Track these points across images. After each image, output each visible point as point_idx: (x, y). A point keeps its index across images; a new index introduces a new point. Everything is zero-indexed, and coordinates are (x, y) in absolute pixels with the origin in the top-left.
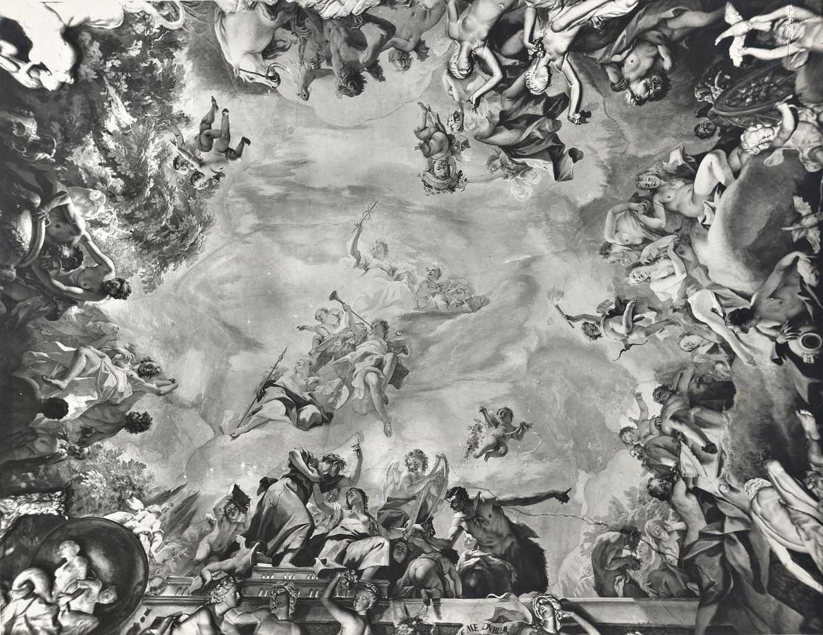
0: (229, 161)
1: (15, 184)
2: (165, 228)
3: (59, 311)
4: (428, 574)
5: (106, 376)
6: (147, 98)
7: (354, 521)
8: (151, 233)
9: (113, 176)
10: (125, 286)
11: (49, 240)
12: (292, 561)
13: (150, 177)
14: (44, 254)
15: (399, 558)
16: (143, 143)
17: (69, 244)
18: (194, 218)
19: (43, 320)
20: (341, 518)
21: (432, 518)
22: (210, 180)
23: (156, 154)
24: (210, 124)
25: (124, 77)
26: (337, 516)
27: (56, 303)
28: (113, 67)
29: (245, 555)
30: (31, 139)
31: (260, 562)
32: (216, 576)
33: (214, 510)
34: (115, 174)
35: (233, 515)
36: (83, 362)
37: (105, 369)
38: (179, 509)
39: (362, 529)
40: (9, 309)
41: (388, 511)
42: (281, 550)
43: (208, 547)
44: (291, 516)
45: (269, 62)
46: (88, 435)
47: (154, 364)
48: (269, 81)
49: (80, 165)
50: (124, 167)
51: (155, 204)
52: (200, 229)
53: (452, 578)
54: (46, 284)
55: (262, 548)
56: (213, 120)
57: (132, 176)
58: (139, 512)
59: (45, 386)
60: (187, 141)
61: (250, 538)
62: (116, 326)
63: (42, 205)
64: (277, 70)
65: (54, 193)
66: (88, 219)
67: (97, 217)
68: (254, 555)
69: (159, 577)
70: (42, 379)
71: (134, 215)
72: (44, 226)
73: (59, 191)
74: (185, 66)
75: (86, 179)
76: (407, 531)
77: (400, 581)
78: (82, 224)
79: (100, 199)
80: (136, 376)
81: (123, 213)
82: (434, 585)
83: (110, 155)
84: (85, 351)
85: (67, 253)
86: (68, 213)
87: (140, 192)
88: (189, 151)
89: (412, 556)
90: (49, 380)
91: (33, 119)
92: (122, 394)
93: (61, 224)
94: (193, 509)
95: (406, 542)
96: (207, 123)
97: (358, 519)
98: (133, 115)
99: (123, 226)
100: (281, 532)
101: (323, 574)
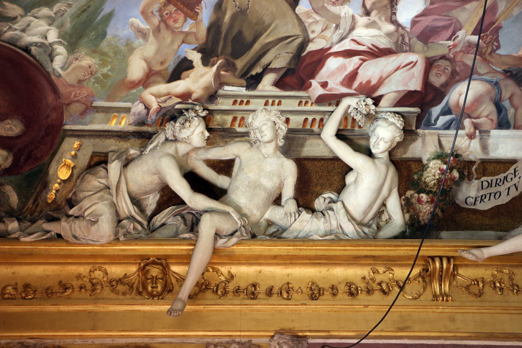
4: (478, 101)
7: (373, 31)
12: (278, 84)
15: (437, 80)
20: (352, 29)
21: (499, 28)
26: (345, 25)
29: (202, 76)
31: (228, 84)
32: (165, 101)
33: (143, 13)
35: (175, 21)
38: (84, 11)
39: (384, 43)
41: (430, 18)
42: (258, 70)
43: (144, 65)
44: (270, 25)
53: (512, 105)
55: (229, 66)
58: (19, 17)
61: (208, 55)
68: (217, 76)
69: (78, 101)
76: (455, 46)
77: (436, 111)
82: (485, 113)
89: (458, 78)
94: (107, 9)
95: (452, 61)
97: (379, 29)
100: (257, 46)
101: (321, 100)
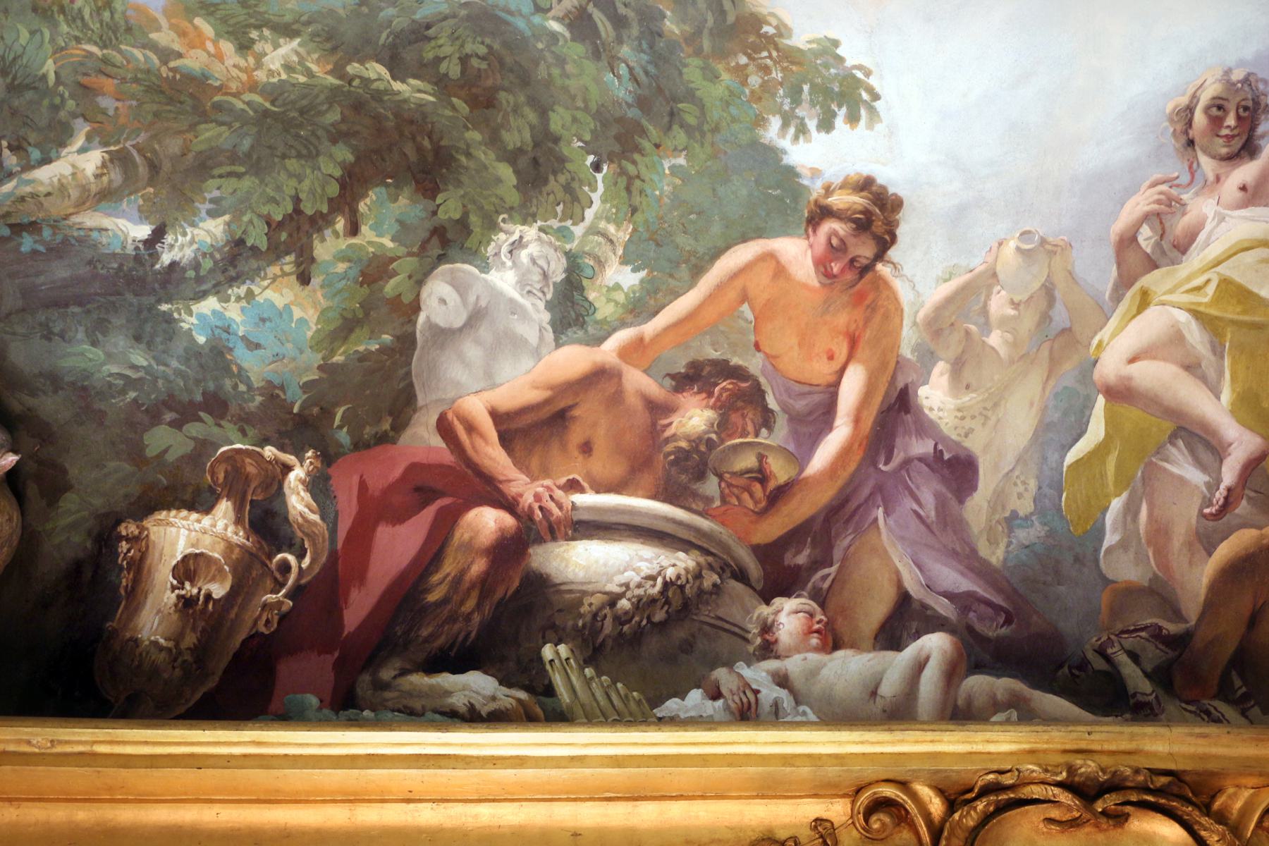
1: (433, 597)
3: (938, 454)
5: (1231, 291)
8: (598, 81)
9: (354, 230)
10: (840, 200)
11: (647, 479)
13: (338, 71)
14: (708, 500)
16: (183, 96)
19: (977, 508)
23: (227, 47)
27: (907, 463)
30: (238, 536)
34: (340, 224)
36: (1156, 375)
37: (1198, 289)
40: (934, 623)
47: (1205, 98)
49: (316, 359)
50: (314, 180)
51: (464, 60)
54: (822, 497)
57: (344, 153)
62: (1012, 244)
63: (508, 505)
65: (448, 458)
66: (550, 335)
67: (541, 305)
70: (1205, 516)
71: (520, 151)
72: (587, 499)
73: (437, 442)
75: (373, 335)
78: (572, 359)
79: (461, 288)
80: (1247, 172)
81: (513, 198)
83: (257, 237)
84: (1111, 366)
87: (412, 122)
90: (1220, 495)
91: (148, 523)
93: (576, 435)
99: (574, 202)
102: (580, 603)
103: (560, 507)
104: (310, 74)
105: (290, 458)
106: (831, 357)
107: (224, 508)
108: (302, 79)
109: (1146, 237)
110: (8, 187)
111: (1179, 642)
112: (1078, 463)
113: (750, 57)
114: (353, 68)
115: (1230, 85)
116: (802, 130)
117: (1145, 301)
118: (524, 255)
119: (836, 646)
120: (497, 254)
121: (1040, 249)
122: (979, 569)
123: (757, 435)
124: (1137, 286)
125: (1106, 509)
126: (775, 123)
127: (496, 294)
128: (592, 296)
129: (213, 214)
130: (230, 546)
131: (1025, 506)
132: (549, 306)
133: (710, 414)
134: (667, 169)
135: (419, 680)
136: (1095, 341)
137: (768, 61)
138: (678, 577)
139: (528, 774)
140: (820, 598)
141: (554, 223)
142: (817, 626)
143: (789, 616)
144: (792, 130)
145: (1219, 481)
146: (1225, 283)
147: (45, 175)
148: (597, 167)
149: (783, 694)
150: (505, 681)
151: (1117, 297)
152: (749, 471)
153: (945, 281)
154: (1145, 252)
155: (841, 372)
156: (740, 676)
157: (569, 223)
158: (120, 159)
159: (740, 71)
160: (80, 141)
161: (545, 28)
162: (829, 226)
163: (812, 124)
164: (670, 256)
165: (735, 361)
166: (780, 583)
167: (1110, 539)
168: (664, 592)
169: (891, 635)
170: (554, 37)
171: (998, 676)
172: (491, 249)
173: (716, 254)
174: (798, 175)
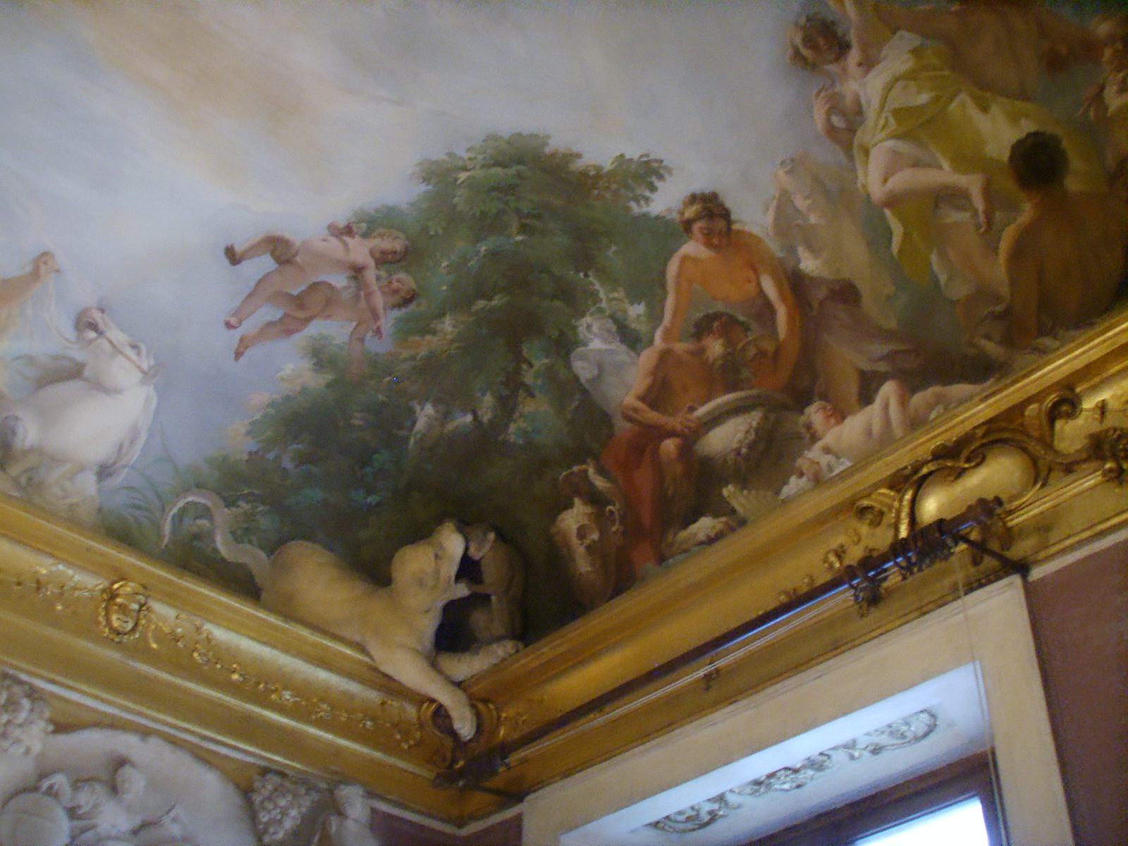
0: (298, 243)
1: (670, 493)
2: (524, 229)
6: (356, 422)
9: (531, 366)
10: (690, 213)
17: (701, 352)
18: (456, 200)
19: (869, 304)
22: (365, 235)
23: (428, 337)
24: (281, 320)
25: (368, 470)
27: (821, 303)
28: (370, 492)
30: (589, 510)
34: (524, 366)
36: (903, 179)
40: (882, 378)
45: (78, 355)
46: (1063, 49)
47: (798, 40)
48: (102, 327)
52: (463, 176)
56: (270, 324)
59: (998, 216)
60: (351, 321)
62: (781, 173)
63: (672, 434)
64: (71, 334)
66: (633, 354)
67: (618, 344)
72: (701, 411)
73: (628, 425)
74: (243, 431)
78: (648, 357)
79: (583, 357)
80: (854, 56)
83: (505, 393)
84: (877, 191)
85: (715, 347)
86: (650, 388)
88: (363, 304)
90: (982, 217)
92: (916, 52)
96: (285, 327)
98: (411, 412)
102: (725, 461)
103: (692, 421)
104: (463, 322)
105: (584, 467)
106: (750, 282)
107: (577, 501)
108: (462, 327)
109: (837, 121)
110: (412, 441)
111: (1007, 312)
112: (900, 251)
113: (595, 189)
114: (474, 308)
115: (803, 28)
116: (647, 200)
117: (866, 152)
118: (595, 329)
119: (844, 418)
120: (585, 336)
121: (794, 166)
122: (889, 336)
123: (747, 337)
124: (855, 146)
125: (931, 264)
126: (633, 205)
127: (600, 351)
128: (633, 326)
129: (484, 394)
130: (589, 516)
131: (890, 289)
132: (622, 341)
133: (720, 341)
134: (611, 254)
135: (683, 534)
136: (859, 184)
137: (606, 184)
138: (759, 423)
139: (944, 428)
140: (824, 397)
141: (593, 309)
142: (830, 413)
143: (815, 414)
144: (642, 202)
145: (976, 211)
146: (897, 113)
147: (421, 424)
148: (586, 275)
149: (829, 458)
150: (716, 515)
151: (851, 157)
152: (757, 354)
153: (768, 210)
154: (845, 127)
155: (759, 285)
156: (809, 459)
157: (598, 305)
158: (436, 402)
159: (599, 197)
160: (418, 408)
161: (516, 242)
162: (697, 226)
163: (647, 193)
164: (648, 288)
165: (711, 311)
166: (802, 400)
167: (943, 278)
168: (757, 434)
169: (866, 398)
170: (522, 241)
171: (926, 388)
172: (581, 336)
173: (663, 273)
174: (664, 217)
